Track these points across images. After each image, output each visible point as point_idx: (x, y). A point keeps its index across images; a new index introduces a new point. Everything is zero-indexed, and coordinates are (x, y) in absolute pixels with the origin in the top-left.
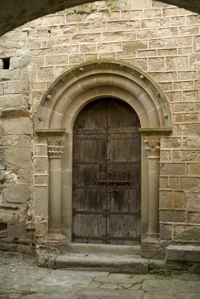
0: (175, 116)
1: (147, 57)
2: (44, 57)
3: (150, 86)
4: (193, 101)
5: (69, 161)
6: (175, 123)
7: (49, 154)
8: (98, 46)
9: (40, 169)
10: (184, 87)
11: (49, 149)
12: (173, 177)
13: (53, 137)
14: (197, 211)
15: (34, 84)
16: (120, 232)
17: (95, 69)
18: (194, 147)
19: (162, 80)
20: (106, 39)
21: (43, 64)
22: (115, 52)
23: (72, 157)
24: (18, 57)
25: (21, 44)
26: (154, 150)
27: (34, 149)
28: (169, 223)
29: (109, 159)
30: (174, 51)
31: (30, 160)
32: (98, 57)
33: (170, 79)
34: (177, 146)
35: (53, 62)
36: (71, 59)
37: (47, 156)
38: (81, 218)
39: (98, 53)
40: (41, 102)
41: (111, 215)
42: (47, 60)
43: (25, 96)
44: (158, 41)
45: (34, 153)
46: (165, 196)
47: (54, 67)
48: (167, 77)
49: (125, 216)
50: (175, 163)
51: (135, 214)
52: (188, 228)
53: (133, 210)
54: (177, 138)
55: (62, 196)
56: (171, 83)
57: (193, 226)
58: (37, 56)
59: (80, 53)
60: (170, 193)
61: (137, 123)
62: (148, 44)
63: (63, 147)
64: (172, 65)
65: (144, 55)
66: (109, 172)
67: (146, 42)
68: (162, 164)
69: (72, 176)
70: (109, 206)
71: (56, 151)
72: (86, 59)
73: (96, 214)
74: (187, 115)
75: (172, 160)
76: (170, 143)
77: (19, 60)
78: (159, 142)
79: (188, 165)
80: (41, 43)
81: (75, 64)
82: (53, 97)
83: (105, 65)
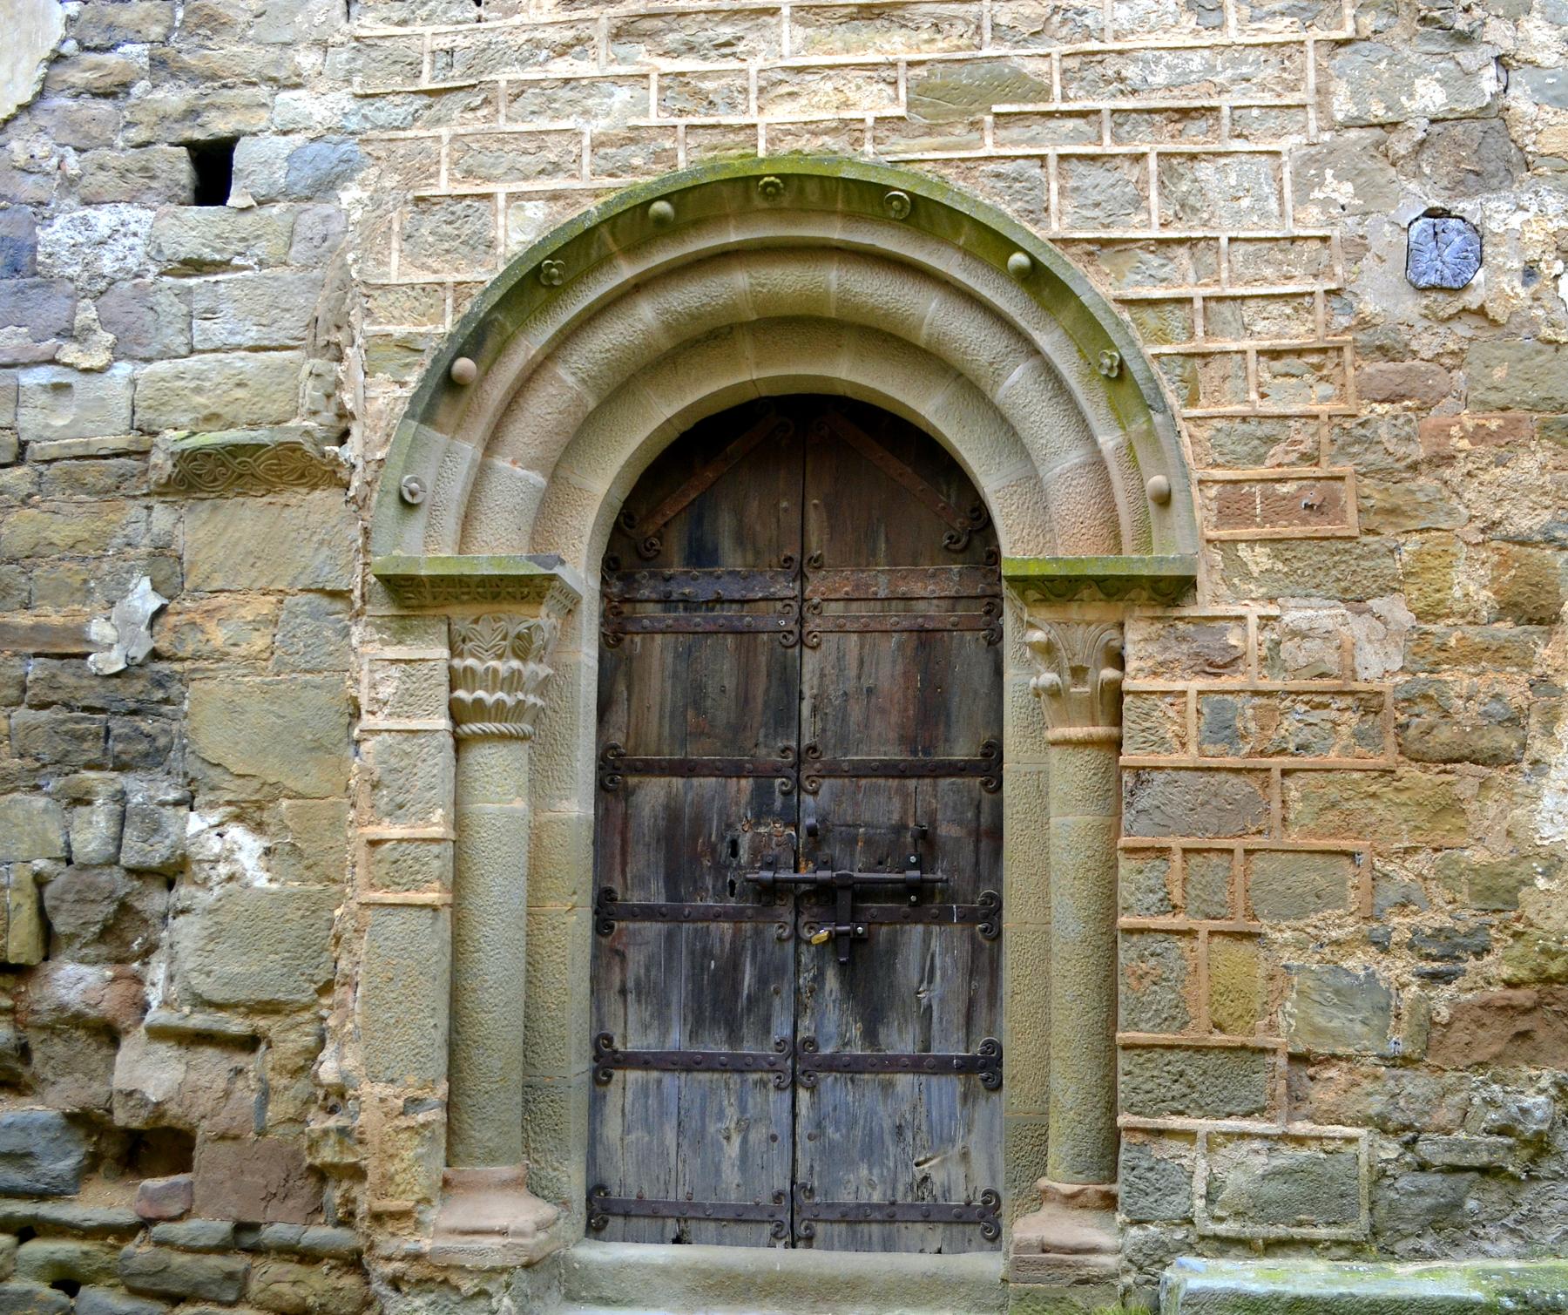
0: (1213, 491)
1: (1051, 151)
2: (438, 139)
3: (1067, 317)
4: (1315, 409)
5: (579, 754)
6: (1212, 534)
7: (457, 713)
8: (764, 83)
9: (399, 799)
10: (1259, 326)
12: (1198, 851)
13: (485, 608)
14: (1340, 1051)
15: (376, 293)
16: (871, 1172)
17: (745, 213)
18: (1321, 676)
19: (1138, 284)
20: (810, 43)
21: (431, 176)
22: (862, 120)
23: (593, 729)
24: (285, 133)
25: (307, 60)
26: (1087, 689)
28: (1176, 1123)
29: (813, 749)
30: (1202, 124)
32: (762, 144)
33: (1182, 278)
34: (1225, 666)
35: (493, 165)
36: (602, 151)
37: (443, 723)
38: (644, 1090)
39: (761, 120)
40: (414, 400)
41: (822, 1075)
42: (456, 155)
43: (319, 364)
44: (1112, 66)
46: (1153, 962)
47: (501, 201)
48: (1167, 269)
49: (904, 1081)
50: (1209, 769)
51: (966, 1067)
52: (1288, 1156)
53: (950, 1046)
54: (1222, 623)
55: (532, 964)
56: (1190, 300)
57: (1319, 1138)
58: (402, 134)
59: (653, 120)
60: (1183, 944)
61: (975, 532)
62: (1057, 77)
63: (544, 670)
64: (1192, 200)
65: (1031, 141)
66: (811, 821)
67: (1043, 66)
68: (1138, 771)
69: (594, 843)
70: (805, 1022)
71: (500, 695)
72: (688, 152)
73: (739, 1066)
74: (1284, 489)
75: (1193, 749)
76: (1185, 647)
77: (287, 152)
78: (1116, 644)
79: (1288, 782)
80: (427, 59)
81: (625, 180)
82: (486, 373)
83: (801, 191)
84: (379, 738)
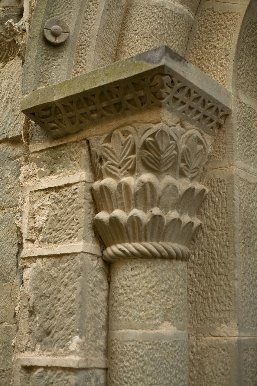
5: (237, 272)
7: (103, 234)
9: (46, 325)
11: (98, 199)
13: (114, 124)
27: (26, 209)
31: (13, 273)
37: (81, 245)
45: (24, 230)
84: (34, 265)
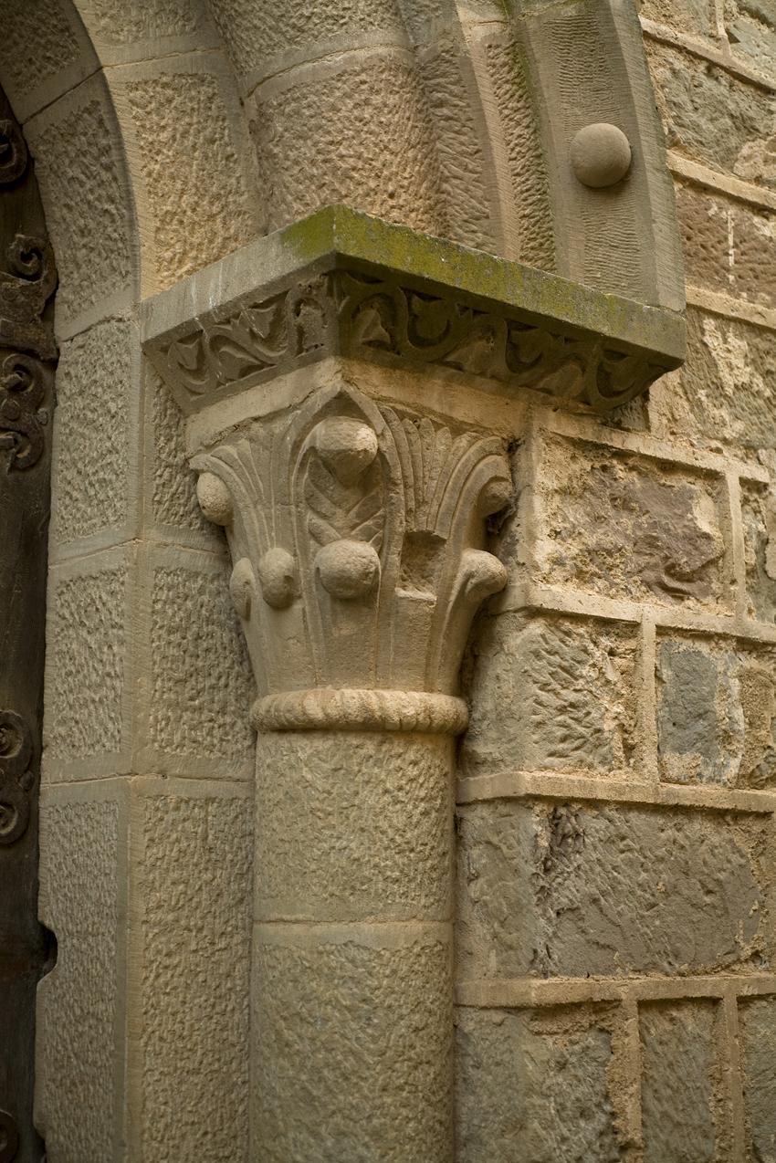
26: (428, 595)
34: (688, 579)
50: (678, 810)
75: (650, 761)
76: (627, 521)
78: (502, 490)
